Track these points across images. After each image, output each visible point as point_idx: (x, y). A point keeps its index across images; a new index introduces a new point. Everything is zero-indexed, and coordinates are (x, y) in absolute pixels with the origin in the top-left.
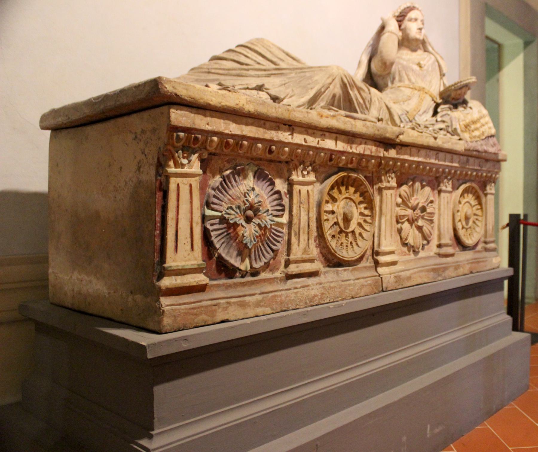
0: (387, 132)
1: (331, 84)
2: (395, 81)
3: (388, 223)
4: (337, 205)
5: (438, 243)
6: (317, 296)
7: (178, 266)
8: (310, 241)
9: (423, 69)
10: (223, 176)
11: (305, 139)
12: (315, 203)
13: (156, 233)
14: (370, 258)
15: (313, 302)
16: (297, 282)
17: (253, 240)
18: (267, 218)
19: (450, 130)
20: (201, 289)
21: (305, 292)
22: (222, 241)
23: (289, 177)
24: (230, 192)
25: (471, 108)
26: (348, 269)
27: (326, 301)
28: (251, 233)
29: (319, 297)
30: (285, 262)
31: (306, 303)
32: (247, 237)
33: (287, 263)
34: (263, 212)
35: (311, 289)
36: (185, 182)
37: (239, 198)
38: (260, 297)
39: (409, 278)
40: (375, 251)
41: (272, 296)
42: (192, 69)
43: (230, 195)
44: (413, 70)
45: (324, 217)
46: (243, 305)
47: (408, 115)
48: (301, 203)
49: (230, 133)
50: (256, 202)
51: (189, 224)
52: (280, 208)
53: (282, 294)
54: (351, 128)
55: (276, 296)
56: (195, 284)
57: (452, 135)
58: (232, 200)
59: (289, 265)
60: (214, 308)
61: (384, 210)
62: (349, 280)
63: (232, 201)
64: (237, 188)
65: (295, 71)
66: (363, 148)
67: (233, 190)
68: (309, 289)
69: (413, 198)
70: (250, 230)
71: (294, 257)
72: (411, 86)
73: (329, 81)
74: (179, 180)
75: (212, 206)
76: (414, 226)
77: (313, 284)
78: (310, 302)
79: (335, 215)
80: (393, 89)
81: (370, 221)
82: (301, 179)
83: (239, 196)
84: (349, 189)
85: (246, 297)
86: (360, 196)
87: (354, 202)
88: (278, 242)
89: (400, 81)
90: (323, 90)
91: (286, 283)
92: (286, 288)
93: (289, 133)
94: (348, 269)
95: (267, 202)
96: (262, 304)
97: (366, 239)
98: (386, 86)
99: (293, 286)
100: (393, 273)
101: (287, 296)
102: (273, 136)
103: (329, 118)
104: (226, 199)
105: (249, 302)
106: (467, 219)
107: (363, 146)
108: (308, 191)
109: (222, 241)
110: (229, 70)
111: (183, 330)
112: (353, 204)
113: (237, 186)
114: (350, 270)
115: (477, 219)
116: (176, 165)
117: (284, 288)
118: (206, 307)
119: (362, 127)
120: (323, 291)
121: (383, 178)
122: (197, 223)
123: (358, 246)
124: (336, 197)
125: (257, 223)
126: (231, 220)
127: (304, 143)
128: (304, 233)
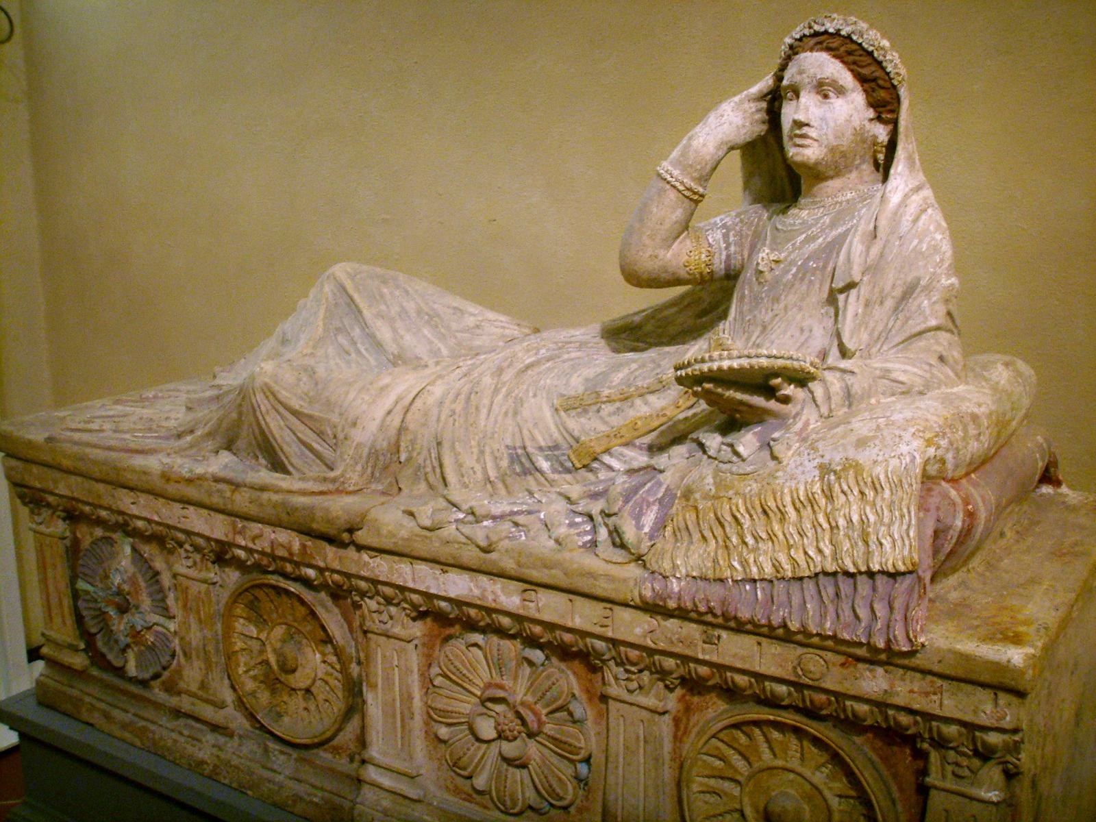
0: (313, 520)
6: (207, 763)
21: (190, 749)
46: (107, 716)
55: (145, 729)
57: (614, 544)
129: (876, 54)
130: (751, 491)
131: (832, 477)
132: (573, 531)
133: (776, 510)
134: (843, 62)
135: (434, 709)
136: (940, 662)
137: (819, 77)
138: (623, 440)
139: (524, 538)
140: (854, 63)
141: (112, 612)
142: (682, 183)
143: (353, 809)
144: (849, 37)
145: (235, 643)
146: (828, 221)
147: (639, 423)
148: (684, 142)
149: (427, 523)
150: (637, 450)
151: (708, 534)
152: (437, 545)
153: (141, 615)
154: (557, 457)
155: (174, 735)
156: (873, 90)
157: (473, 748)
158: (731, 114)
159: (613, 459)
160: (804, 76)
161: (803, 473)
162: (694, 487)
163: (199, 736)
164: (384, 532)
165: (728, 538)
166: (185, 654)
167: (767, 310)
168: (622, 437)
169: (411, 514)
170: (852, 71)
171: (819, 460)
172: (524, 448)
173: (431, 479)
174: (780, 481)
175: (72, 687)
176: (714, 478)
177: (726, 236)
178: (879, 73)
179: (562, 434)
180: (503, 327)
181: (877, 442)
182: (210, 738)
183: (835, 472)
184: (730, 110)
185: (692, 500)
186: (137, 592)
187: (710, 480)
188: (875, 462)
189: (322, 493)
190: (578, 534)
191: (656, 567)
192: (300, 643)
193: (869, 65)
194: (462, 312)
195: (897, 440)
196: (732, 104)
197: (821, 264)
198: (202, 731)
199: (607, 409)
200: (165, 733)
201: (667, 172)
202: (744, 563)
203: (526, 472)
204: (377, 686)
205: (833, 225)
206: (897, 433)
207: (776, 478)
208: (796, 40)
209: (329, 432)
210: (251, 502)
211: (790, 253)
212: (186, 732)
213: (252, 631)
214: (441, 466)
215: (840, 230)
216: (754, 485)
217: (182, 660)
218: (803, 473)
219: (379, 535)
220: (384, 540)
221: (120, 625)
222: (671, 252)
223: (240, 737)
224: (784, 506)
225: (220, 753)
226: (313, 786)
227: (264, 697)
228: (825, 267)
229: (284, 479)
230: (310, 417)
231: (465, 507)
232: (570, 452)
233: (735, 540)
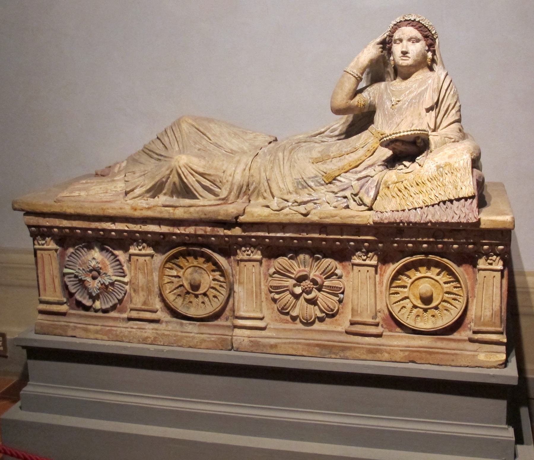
0: (219, 215)
1: (170, 174)
6: (150, 338)
7: (45, 299)
11: (126, 226)
15: (146, 341)
17: (95, 291)
18: (106, 278)
20: (64, 314)
21: (139, 333)
22: (78, 288)
26: (195, 324)
27: (159, 344)
31: (139, 341)
32: (91, 289)
34: (102, 273)
35: (144, 331)
38: (99, 328)
39: (272, 346)
41: (109, 330)
45: (166, 279)
48: (139, 269)
49: (64, 226)
52: (121, 271)
54: (169, 216)
56: (56, 311)
57: (358, 205)
60: (66, 327)
62: (191, 333)
66: (194, 230)
67: (83, 258)
68: (142, 332)
71: (134, 306)
73: (168, 172)
74: (42, 252)
75: (67, 266)
77: (149, 329)
78: (143, 340)
79: (181, 279)
81: (225, 287)
82: (137, 252)
84: (198, 259)
85: (91, 326)
87: (205, 270)
88: (122, 294)
90: (164, 180)
91: (127, 323)
92: (124, 326)
93: (110, 223)
94: (195, 324)
95: (109, 266)
99: (132, 326)
100: (252, 337)
101: (121, 332)
102: (97, 226)
103: (144, 210)
104: (78, 263)
107: (193, 228)
108: (145, 261)
109: (78, 288)
111: (47, 335)
112: (203, 272)
114: (197, 325)
116: (39, 244)
118: (61, 326)
119: (183, 214)
120: (156, 335)
121: (238, 251)
122: (56, 277)
124: (182, 265)
125: (99, 280)
126: (80, 276)
127: (126, 229)
129: (428, 27)
130: (411, 178)
131: (441, 169)
132: (339, 203)
133: (421, 183)
134: (418, 30)
135: (271, 287)
136: (484, 224)
137: (411, 35)
138: (346, 170)
139: (319, 208)
140: (422, 31)
141: (89, 279)
142: (357, 75)
143: (232, 339)
144: (419, 22)
145: (164, 280)
146: (417, 86)
147: (351, 163)
148: (356, 59)
149: (277, 208)
150: (351, 174)
151: (395, 195)
152: (282, 216)
153: (108, 277)
154: (317, 180)
155: (129, 330)
156: (428, 40)
157: (291, 300)
158: (372, 49)
159: (342, 178)
160: (405, 35)
161: (431, 169)
162: (388, 180)
163: (143, 327)
164: (256, 215)
165: (404, 195)
166: (135, 291)
167: (398, 119)
168: (345, 169)
169: (268, 207)
170: (421, 33)
171: (436, 164)
172: (303, 178)
173: (265, 195)
174: (422, 173)
175: (60, 321)
176: (396, 176)
177: (369, 94)
178: (430, 34)
179: (317, 171)
180: (264, 137)
181: (455, 156)
183: (442, 167)
184: (371, 48)
185: (387, 185)
186: (105, 267)
187: (394, 176)
188: (456, 162)
189: (218, 205)
190: (342, 203)
191: (378, 210)
192: (201, 273)
193: (427, 31)
194: (246, 133)
195: (462, 154)
196: (372, 46)
197: (417, 101)
198: (143, 325)
199: (334, 160)
200: (124, 329)
201: (350, 71)
202: (412, 203)
203: (304, 187)
204: (243, 283)
205: (420, 86)
206: (461, 152)
207: (420, 172)
208: (398, 22)
209: (218, 180)
210: (185, 213)
211: (404, 98)
213: (174, 273)
214: (270, 188)
215: (423, 88)
216: (412, 176)
217: (133, 294)
218: (431, 169)
219: (253, 216)
220: (254, 218)
221: (94, 285)
222: (352, 101)
224: (425, 181)
225: (157, 332)
226: (210, 334)
227: (180, 301)
228: (419, 101)
229: (199, 202)
230: (209, 175)
231: (292, 200)
232: (323, 178)
233: (407, 195)
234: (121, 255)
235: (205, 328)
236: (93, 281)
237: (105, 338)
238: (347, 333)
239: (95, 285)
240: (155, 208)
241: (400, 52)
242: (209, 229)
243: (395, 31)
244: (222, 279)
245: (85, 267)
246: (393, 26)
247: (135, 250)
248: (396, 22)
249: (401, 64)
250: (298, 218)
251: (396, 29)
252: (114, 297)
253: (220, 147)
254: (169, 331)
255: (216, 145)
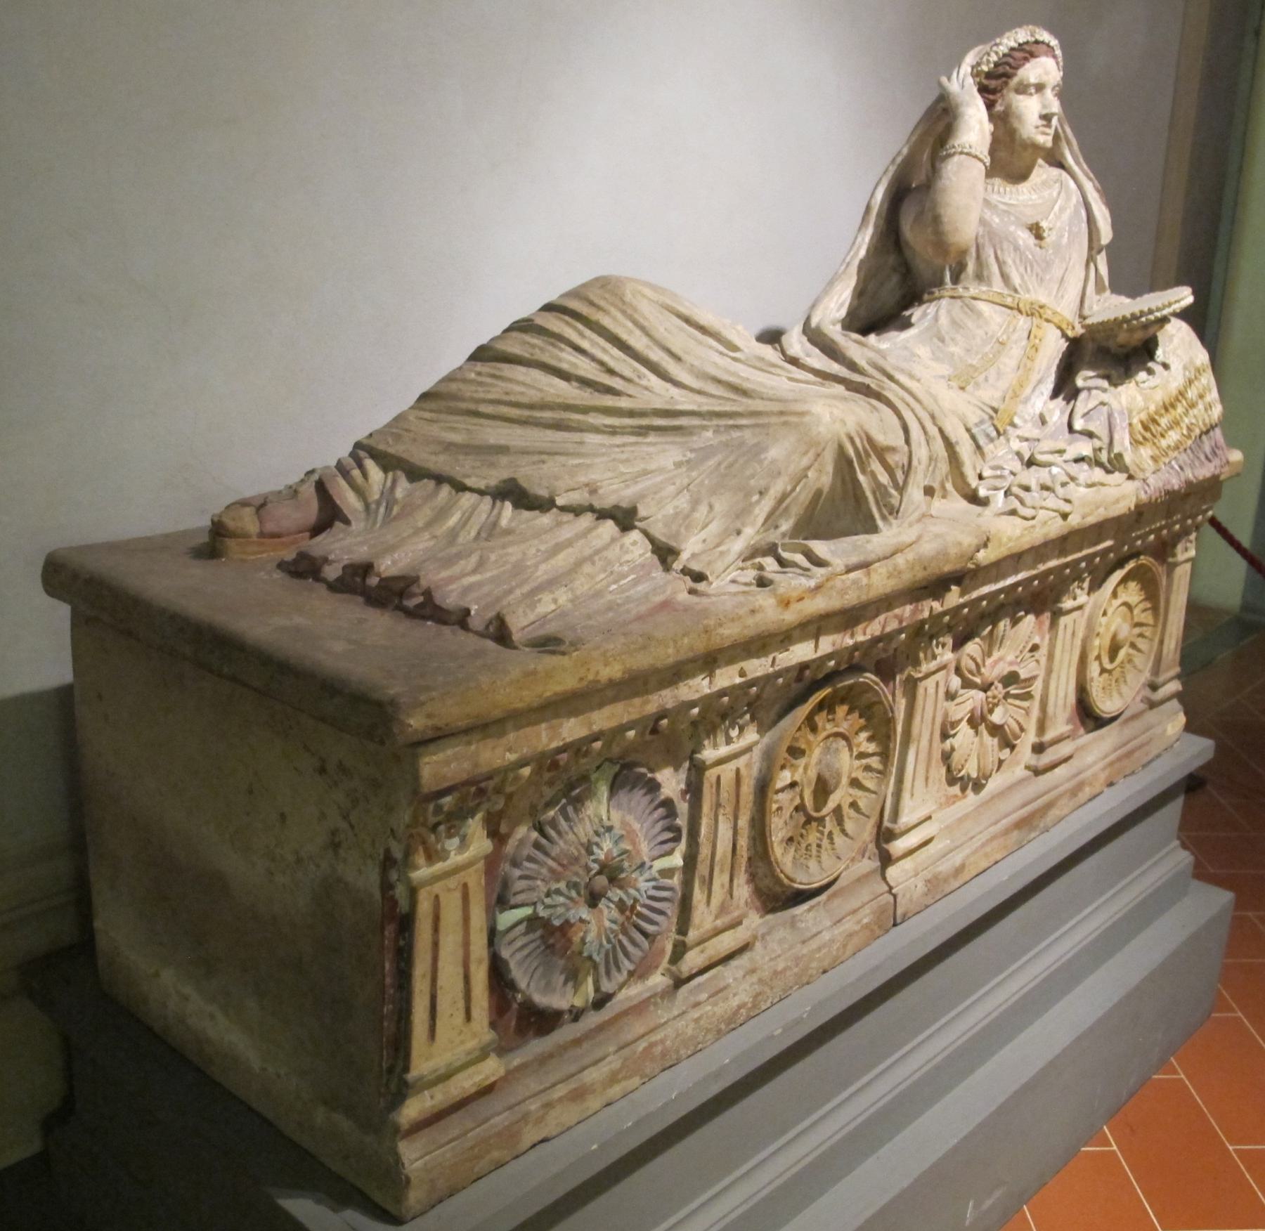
1: (809, 468)
2: (963, 276)
3: (923, 756)
4: (803, 765)
5: (1037, 740)
8: (735, 882)
9: (1043, 243)
10: (539, 823)
12: (752, 782)
13: (385, 1010)
14: (872, 847)
16: (699, 985)
17: (605, 942)
19: (1104, 457)
22: (535, 964)
23: (694, 752)
24: (555, 851)
25: (1166, 366)
27: (764, 1007)
28: (602, 929)
29: (750, 1005)
30: (675, 946)
31: (719, 1031)
33: (677, 955)
36: (452, 886)
37: (577, 859)
39: (959, 870)
40: (883, 829)
42: (425, 397)
43: (553, 859)
44: (1017, 248)
47: (996, 422)
50: (615, 855)
51: (461, 970)
53: (665, 1035)
57: (1108, 472)
58: (559, 869)
59: (683, 953)
61: (915, 731)
63: (559, 873)
64: (571, 836)
65: (715, 422)
67: (561, 843)
69: (989, 661)
70: (600, 921)
72: (1009, 301)
76: (982, 728)
80: (959, 302)
82: (724, 750)
83: (576, 854)
84: (835, 713)
86: (861, 717)
88: (661, 913)
89: (980, 277)
92: (676, 1013)
93: (703, 676)
96: (620, 1076)
97: (867, 813)
98: (940, 283)
99: (692, 999)
101: (678, 1035)
105: (592, 1085)
106: (1114, 650)
110: (531, 407)
113: (571, 828)
115: (1141, 635)
117: (671, 1016)
123: (846, 835)
128: (722, 871)
155: (695, 1014)
163: (722, 985)
166: (703, 881)
182: (728, 973)
200: (681, 1024)
208: (1020, 45)
212: (704, 996)
223: (763, 936)
234: (671, 782)
235: (836, 902)
236: (595, 911)
237: (636, 1081)
238: (1037, 772)
239: (607, 924)
240: (829, 584)
241: (1036, 116)
242: (908, 609)
243: (1024, 64)
244: (872, 747)
245: (577, 874)
246: (1006, 51)
247: (715, 746)
248: (1015, 41)
249: (1044, 143)
250: (1056, 527)
251: (1026, 59)
252: (638, 937)
253: (772, 370)
254: (779, 956)
255: (758, 364)
